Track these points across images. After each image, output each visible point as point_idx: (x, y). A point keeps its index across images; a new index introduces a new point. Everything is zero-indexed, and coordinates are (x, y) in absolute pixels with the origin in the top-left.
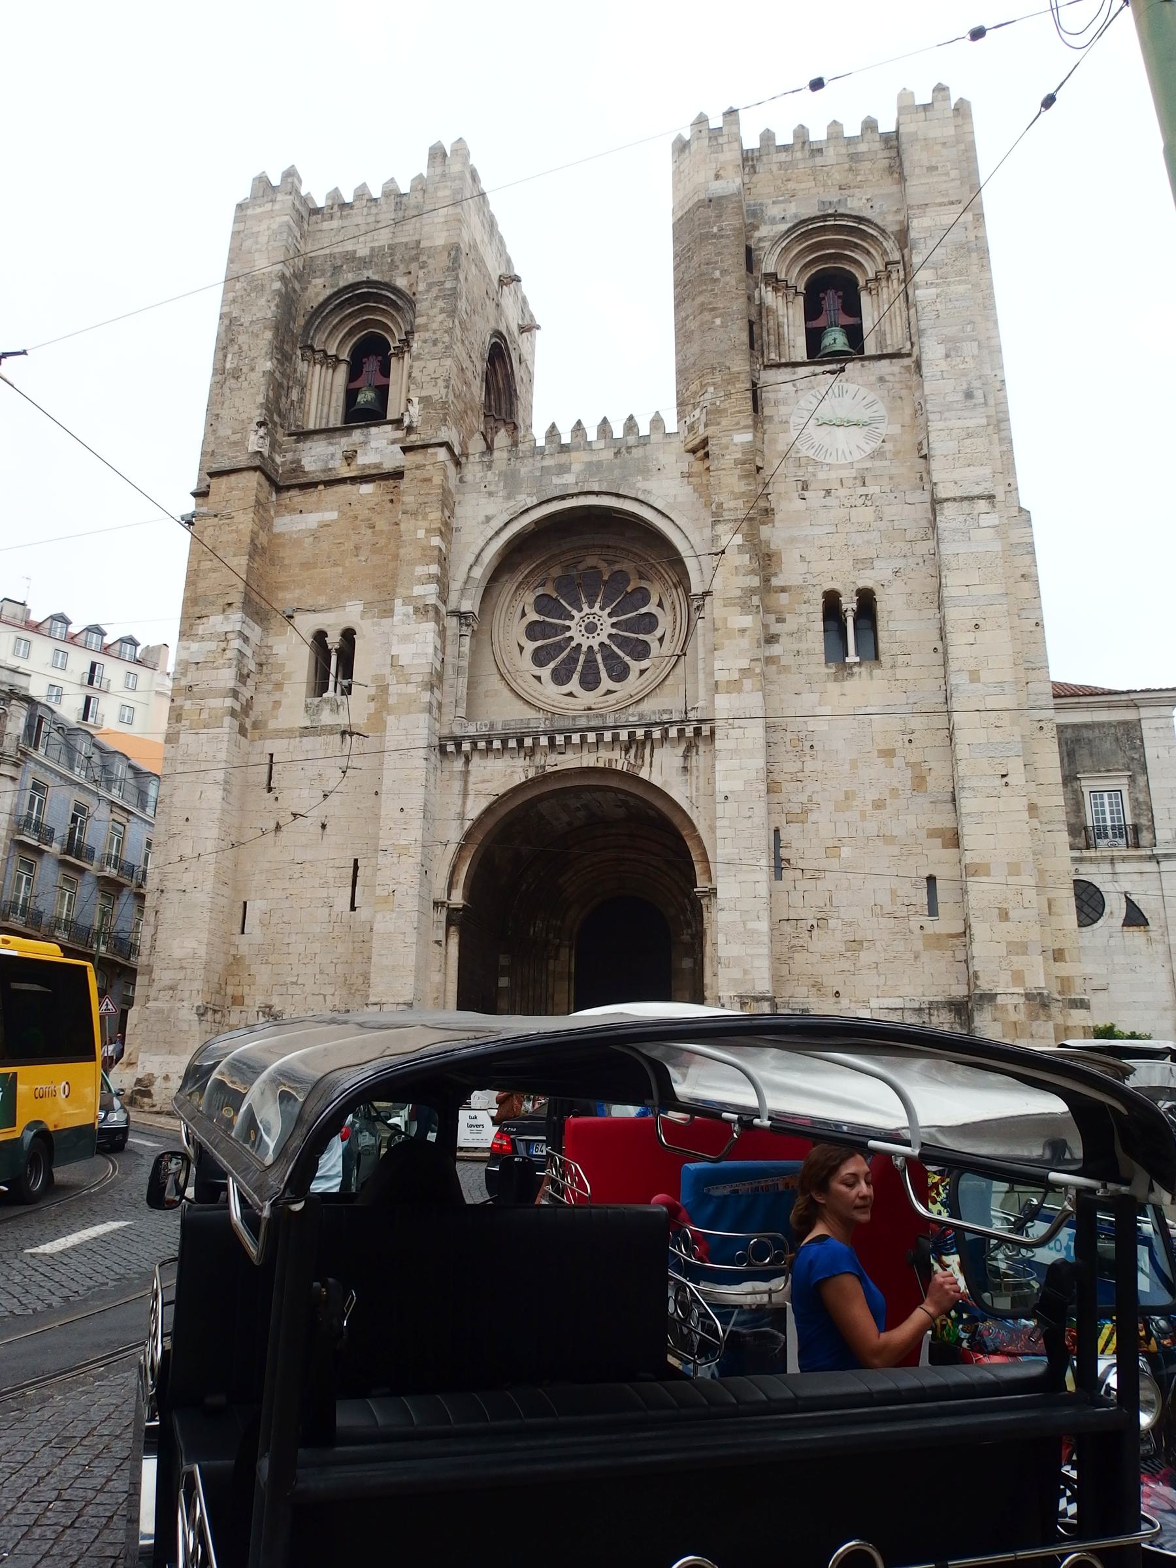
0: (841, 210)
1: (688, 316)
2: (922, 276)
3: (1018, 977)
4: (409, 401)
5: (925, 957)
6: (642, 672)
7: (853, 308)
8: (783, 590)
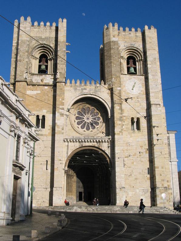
0: (134, 46)
1: (108, 63)
2: (149, 62)
3: (163, 185)
4: (57, 73)
5: (147, 181)
6: (97, 128)
7: (135, 64)
8: (125, 116)
